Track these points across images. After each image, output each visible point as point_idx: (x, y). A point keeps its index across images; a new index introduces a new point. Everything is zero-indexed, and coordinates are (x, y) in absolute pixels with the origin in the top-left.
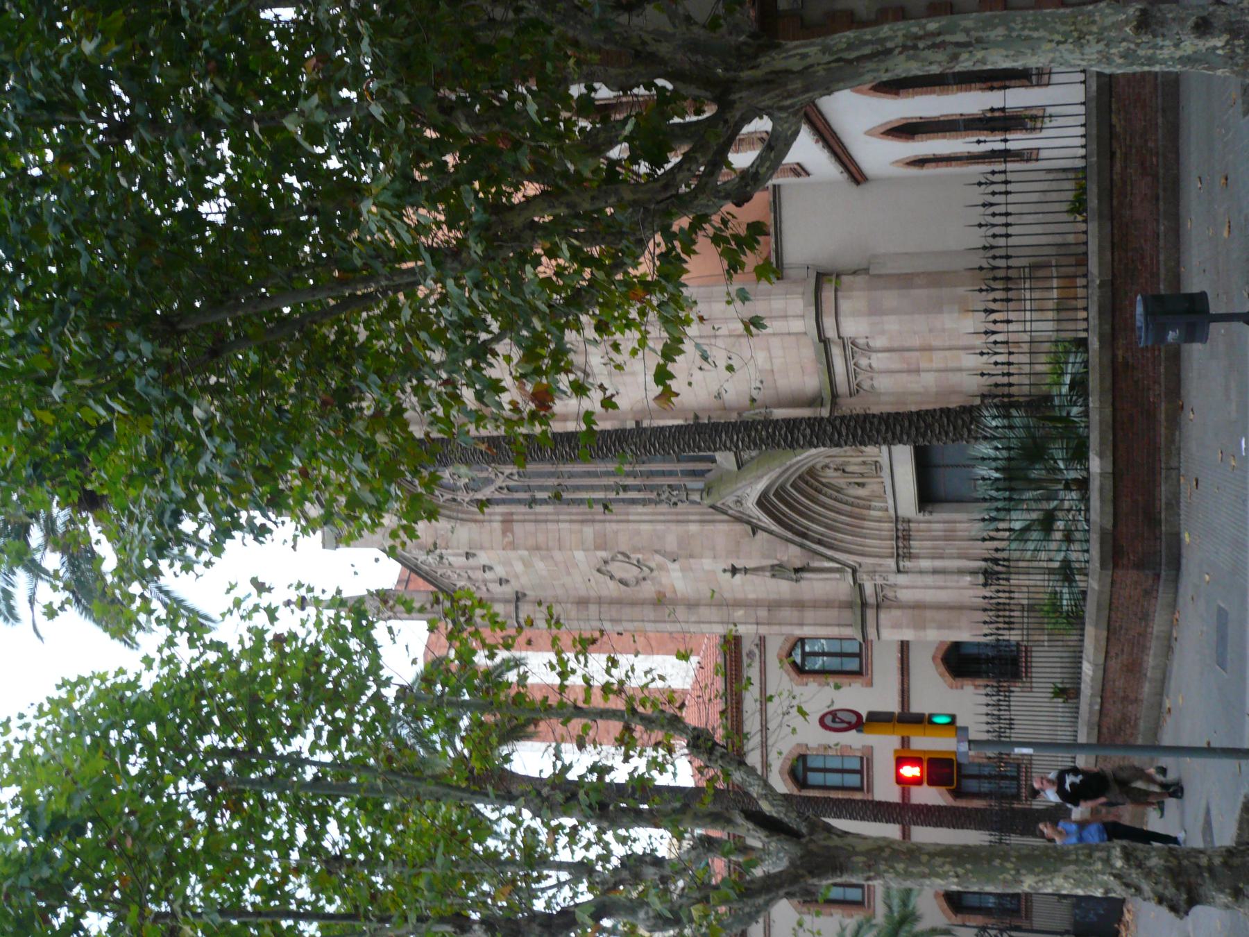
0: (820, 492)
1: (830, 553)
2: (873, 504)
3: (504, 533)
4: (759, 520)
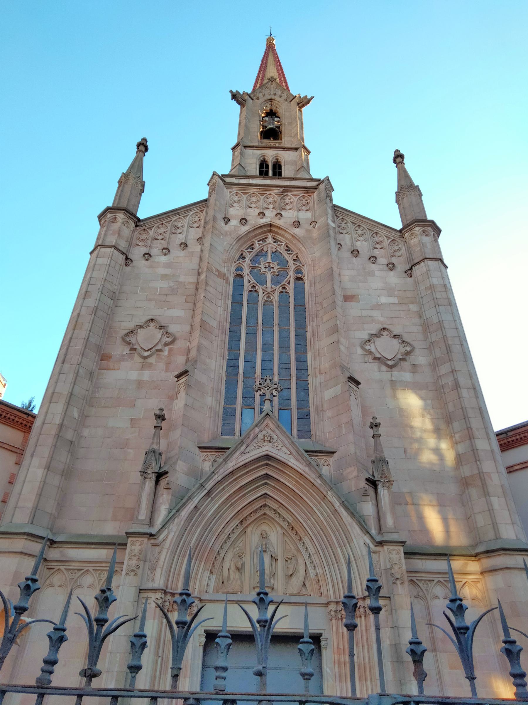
2: (214, 577)
4: (243, 453)
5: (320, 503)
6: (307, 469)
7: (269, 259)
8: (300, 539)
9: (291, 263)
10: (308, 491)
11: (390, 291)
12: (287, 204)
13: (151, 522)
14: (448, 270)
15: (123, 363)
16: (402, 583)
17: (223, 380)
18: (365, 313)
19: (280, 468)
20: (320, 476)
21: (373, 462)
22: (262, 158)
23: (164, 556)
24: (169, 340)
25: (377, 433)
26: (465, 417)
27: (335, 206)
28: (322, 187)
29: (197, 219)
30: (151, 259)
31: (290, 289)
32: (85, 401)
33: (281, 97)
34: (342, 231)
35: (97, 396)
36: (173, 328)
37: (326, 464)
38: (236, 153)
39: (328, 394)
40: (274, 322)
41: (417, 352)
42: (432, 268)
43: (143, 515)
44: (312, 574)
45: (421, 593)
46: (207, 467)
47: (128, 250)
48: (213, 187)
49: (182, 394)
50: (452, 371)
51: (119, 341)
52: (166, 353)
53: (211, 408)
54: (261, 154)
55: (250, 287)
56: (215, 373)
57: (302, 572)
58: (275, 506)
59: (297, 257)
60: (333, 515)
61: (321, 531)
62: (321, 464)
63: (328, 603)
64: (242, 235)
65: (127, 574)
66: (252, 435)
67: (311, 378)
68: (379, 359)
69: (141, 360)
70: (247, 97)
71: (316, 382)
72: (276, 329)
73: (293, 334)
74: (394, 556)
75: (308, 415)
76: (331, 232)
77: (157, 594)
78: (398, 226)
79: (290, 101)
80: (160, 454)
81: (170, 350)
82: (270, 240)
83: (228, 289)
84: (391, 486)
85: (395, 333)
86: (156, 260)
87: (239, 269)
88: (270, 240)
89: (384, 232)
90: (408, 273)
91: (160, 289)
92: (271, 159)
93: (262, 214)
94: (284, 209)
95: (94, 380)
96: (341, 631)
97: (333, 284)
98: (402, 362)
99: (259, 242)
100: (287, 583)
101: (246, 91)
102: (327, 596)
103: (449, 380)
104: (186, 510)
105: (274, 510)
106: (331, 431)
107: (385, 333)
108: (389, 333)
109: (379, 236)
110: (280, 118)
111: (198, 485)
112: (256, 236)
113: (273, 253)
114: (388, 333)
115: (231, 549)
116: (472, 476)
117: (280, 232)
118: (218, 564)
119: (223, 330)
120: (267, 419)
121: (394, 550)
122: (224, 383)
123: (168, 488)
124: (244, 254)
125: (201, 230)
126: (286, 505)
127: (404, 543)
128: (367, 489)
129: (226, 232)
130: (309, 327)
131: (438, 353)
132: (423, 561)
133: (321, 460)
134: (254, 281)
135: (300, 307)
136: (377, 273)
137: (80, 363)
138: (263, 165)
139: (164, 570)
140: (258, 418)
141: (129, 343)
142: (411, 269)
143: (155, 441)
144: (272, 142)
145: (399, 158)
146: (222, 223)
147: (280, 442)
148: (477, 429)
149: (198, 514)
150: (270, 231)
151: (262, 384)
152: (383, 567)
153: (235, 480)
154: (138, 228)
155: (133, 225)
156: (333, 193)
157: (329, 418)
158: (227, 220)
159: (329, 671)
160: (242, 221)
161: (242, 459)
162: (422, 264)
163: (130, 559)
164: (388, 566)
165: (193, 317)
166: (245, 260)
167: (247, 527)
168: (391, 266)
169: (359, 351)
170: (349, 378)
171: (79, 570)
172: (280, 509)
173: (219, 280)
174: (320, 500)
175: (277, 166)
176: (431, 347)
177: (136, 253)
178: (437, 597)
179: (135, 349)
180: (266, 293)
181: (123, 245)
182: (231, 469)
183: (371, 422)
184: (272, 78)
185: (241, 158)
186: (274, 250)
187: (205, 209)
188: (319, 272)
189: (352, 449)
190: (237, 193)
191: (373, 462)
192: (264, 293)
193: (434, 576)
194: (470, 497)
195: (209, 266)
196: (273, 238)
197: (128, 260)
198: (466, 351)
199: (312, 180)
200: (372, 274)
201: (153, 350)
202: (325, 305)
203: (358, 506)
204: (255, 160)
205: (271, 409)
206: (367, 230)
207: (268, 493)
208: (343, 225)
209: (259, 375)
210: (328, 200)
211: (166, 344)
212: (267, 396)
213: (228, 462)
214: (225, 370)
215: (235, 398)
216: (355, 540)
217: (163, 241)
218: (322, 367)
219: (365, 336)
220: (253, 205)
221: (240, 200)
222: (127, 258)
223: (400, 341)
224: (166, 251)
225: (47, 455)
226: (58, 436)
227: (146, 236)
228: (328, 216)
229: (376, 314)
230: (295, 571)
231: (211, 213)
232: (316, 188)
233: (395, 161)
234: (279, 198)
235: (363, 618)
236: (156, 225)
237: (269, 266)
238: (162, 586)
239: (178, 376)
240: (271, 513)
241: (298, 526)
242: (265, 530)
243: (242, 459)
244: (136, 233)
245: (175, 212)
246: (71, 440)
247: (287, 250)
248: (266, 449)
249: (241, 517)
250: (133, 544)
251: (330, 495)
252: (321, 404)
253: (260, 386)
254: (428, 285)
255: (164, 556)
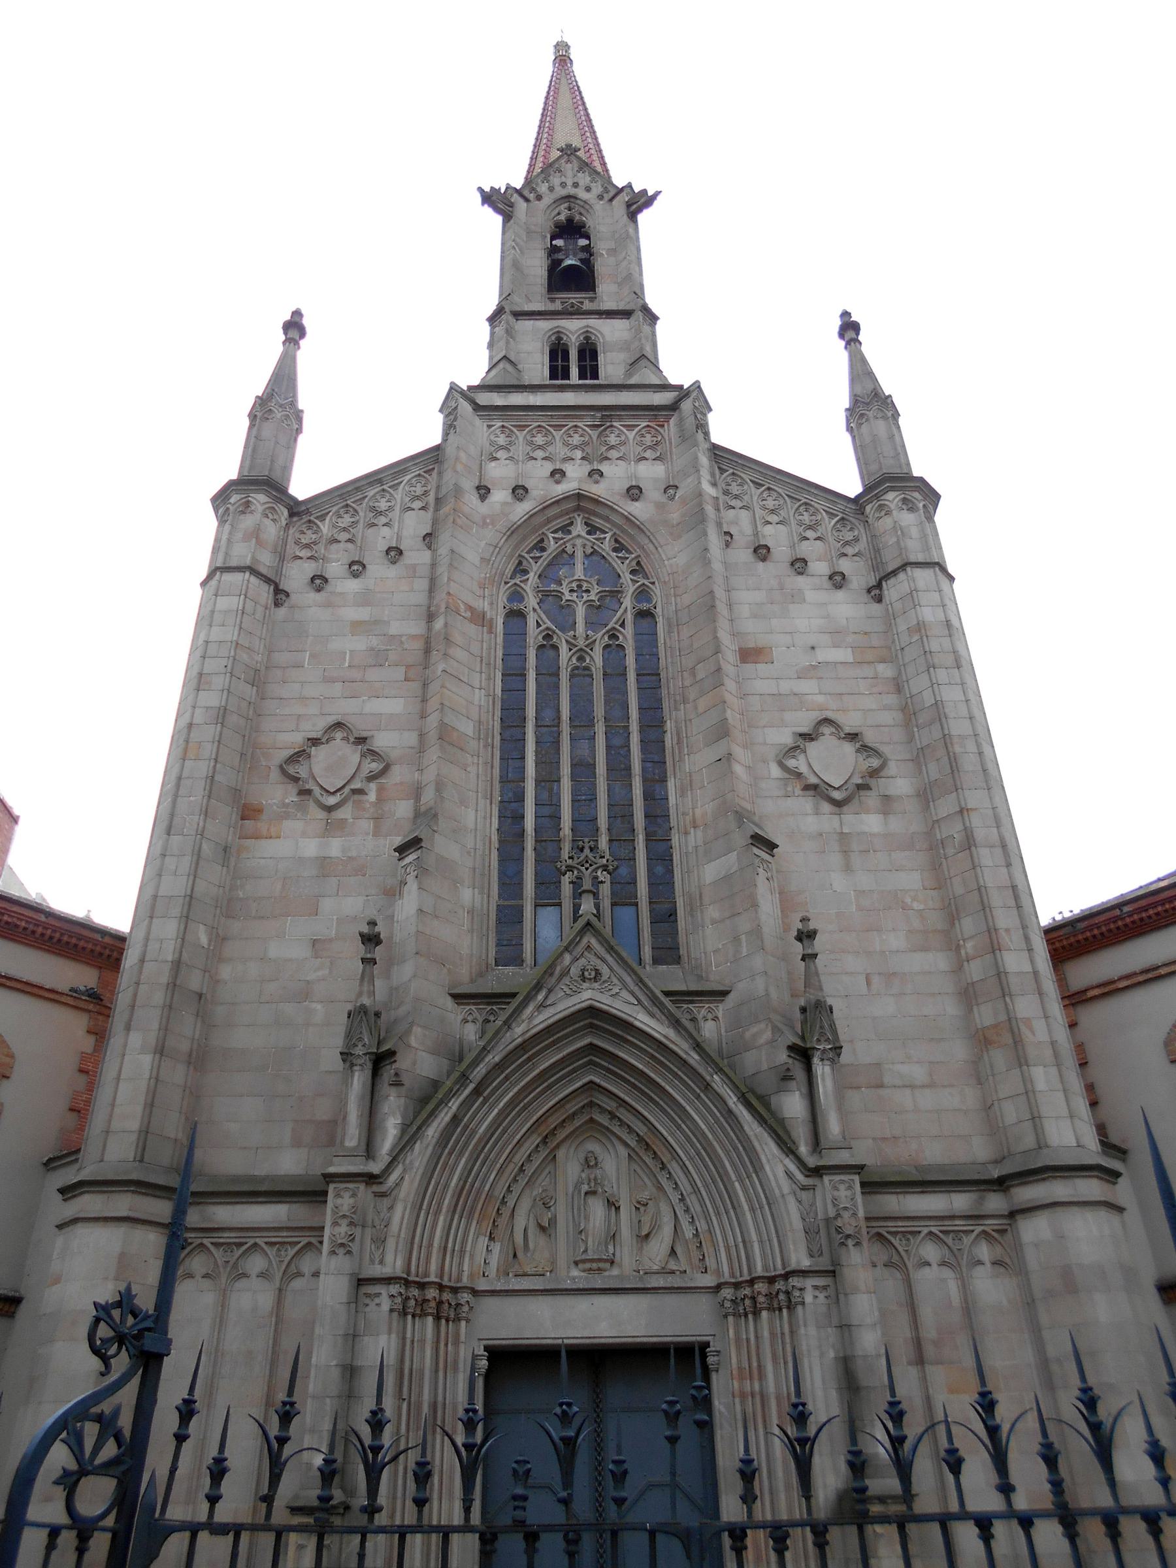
0: (545, 1141)
1: (432, 1132)
2: (496, 1248)
3: (470, 608)
4: (542, 1006)
5: (698, 1097)
6: (671, 1033)
7: (579, 573)
8: (663, 1167)
9: (626, 577)
10: (676, 1075)
11: (837, 634)
12: (612, 447)
13: (369, 1151)
14: (956, 585)
15: (287, 824)
16: (858, 1244)
17: (493, 848)
18: (785, 686)
19: (619, 1032)
20: (698, 1046)
21: (803, 1010)
22: (553, 338)
23: (400, 1216)
24: (376, 766)
25: (810, 951)
26: (985, 908)
27: (715, 447)
28: (686, 406)
29: (419, 490)
30: (329, 588)
31: (628, 637)
32: (218, 911)
33: (588, 189)
34: (733, 503)
35: (241, 896)
36: (383, 741)
37: (710, 1016)
38: (497, 329)
39: (711, 872)
40: (595, 714)
41: (892, 768)
42: (921, 584)
43: (353, 1136)
44: (688, 1232)
45: (895, 1258)
46: (471, 1033)
47: (279, 571)
48: (452, 417)
49: (412, 886)
50: (961, 811)
51: (275, 775)
52: (372, 797)
53: (471, 912)
54: (551, 330)
55: (540, 637)
56: (475, 836)
57: (667, 1231)
58: (610, 1105)
59: (638, 563)
60: (724, 1118)
61: (702, 1151)
62: (700, 1017)
63: (718, 1288)
64: (519, 523)
65: (333, 1253)
66: (558, 968)
67: (677, 835)
68: (815, 787)
69: (321, 814)
70: (516, 198)
71: (687, 847)
72: (600, 729)
73: (635, 739)
74: (843, 1193)
75: (672, 914)
76: (709, 509)
77: (391, 1287)
78: (851, 486)
79: (611, 200)
80: (377, 1015)
81: (381, 790)
82: (579, 529)
83: (493, 645)
84: (836, 1059)
85: (847, 730)
86: (339, 590)
87: (516, 595)
88: (579, 529)
89: (820, 504)
90: (873, 594)
91: (350, 655)
92: (573, 338)
93: (558, 474)
94: (607, 458)
95: (233, 860)
96: (744, 1337)
97: (715, 631)
98: (862, 793)
99: (556, 536)
100: (640, 1249)
101: (513, 185)
102: (718, 1272)
103: (954, 830)
104: (435, 1124)
105: (610, 1113)
106: (719, 949)
107: (827, 730)
108: (837, 729)
109: (812, 510)
110: (588, 238)
111: (457, 1074)
112: (549, 521)
113: (586, 556)
114: (834, 730)
115: (527, 1192)
116: (995, 1026)
117: (599, 510)
118: (503, 1221)
119: (487, 739)
120: (588, 934)
121: (842, 1182)
122: (495, 855)
123: (397, 1084)
124: (525, 563)
125: (428, 515)
126: (633, 1103)
127: (862, 1167)
128: (791, 1067)
129: (484, 518)
130: (668, 722)
131: (933, 771)
132: (901, 1197)
133: (701, 1010)
134: (549, 624)
135: (650, 677)
136: (810, 595)
137: (203, 831)
138: (558, 353)
139: (401, 1240)
140: (569, 934)
141: (296, 780)
142: (879, 586)
143: (365, 989)
144: (574, 297)
145: (849, 329)
146: (472, 498)
147: (615, 981)
148: (1007, 930)
149: (459, 1129)
150: (578, 508)
151: (575, 859)
152: (820, 1216)
153: (529, 1059)
154: (295, 519)
155: (286, 513)
156: (711, 418)
157: (714, 922)
158: (483, 491)
159: (723, 1409)
160: (517, 492)
161: (541, 1018)
162: (901, 576)
163: (335, 1224)
164: (832, 1213)
165: (423, 716)
166: (526, 577)
167: (558, 1146)
168: (838, 580)
169: (775, 771)
170: (752, 837)
171: (240, 1245)
172: (622, 1110)
173: (472, 630)
174: (698, 1091)
175: (589, 354)
176: (919, 758)
177: (296, 576)
178: (928, 1264)
179: (308, 792)
180: (575, 650)
181: (266, 561)
182: (520, 1040)
183: (799, 930)
184: (569, 146)
185: (508, 343)
186: (589, 551)
187: (436, 466)
188: (686, 599)
189: (760, 984)
190: (503, 426)
191: (803, 1010)
192: (570, 650)
193: (923, 1223)
194: (992, 1067)
195: (450, 601)
196: (586, 524)
197: (280, 595)
198: (990, 766)
199: (665, 387)
200: (796, 597)
201: (346, 790)
202: (701, 675)
203: (774, 1100)
204: (539, 345)
205: (595, 912)
206: (786, 498)
207: (597, 1080)
208: (735, 489)
209: (567, 833)
210: (700, 436)
211: (371, 778)
212: (587, 885)
213: (514, 1025)
214: (497, 826)
215: (520, 884)
216: (767, 1168)
217: (350, 545)
218: (698, 812)
219: (786, 738)
220: (540, 454)
221: (510, 443)
222: (278, 591)
223: (858, 745)
224: (357, 568)
225: (156, 1026)
226: (173, 986)
227: (314, 536)
228: (701, 473)
229: (807, 686)
230: (655, 1227)
231: (448, 477)
232: (674, 407)
233: (841, 335)
234: (594, 434)
235: (785, 1311)
236: (334, 509)
237: (580, 586)
238: (399, 1271)
239: (402, 850)
240: (604, 1120)
241: (658, 1142)
242: (592, 1152)
243: (541, 1018)
244: (291, 531)
245: (375, 479)
246: (199, 991)
247: (615, 550)
248: (587, 995)
249: (544, 1130)
250: (338, 1195)
251: (717, 1081)
252: (698, 893)
253: (570, 862)
254: (915, 622)
255: (400, 1216)
